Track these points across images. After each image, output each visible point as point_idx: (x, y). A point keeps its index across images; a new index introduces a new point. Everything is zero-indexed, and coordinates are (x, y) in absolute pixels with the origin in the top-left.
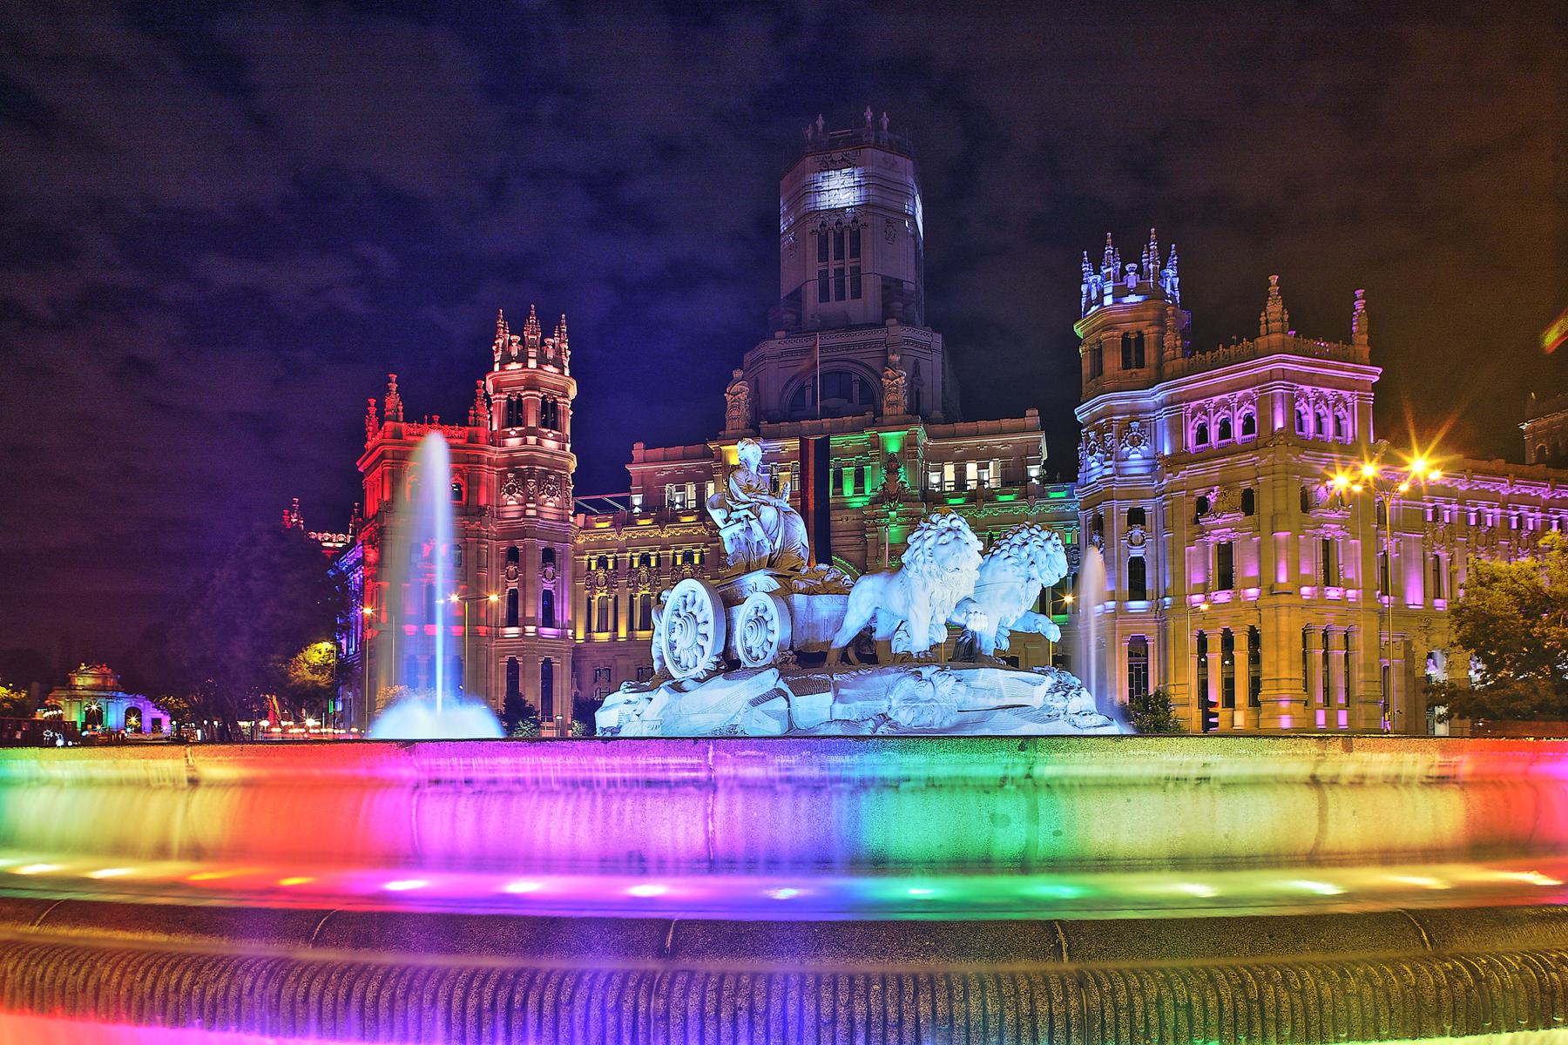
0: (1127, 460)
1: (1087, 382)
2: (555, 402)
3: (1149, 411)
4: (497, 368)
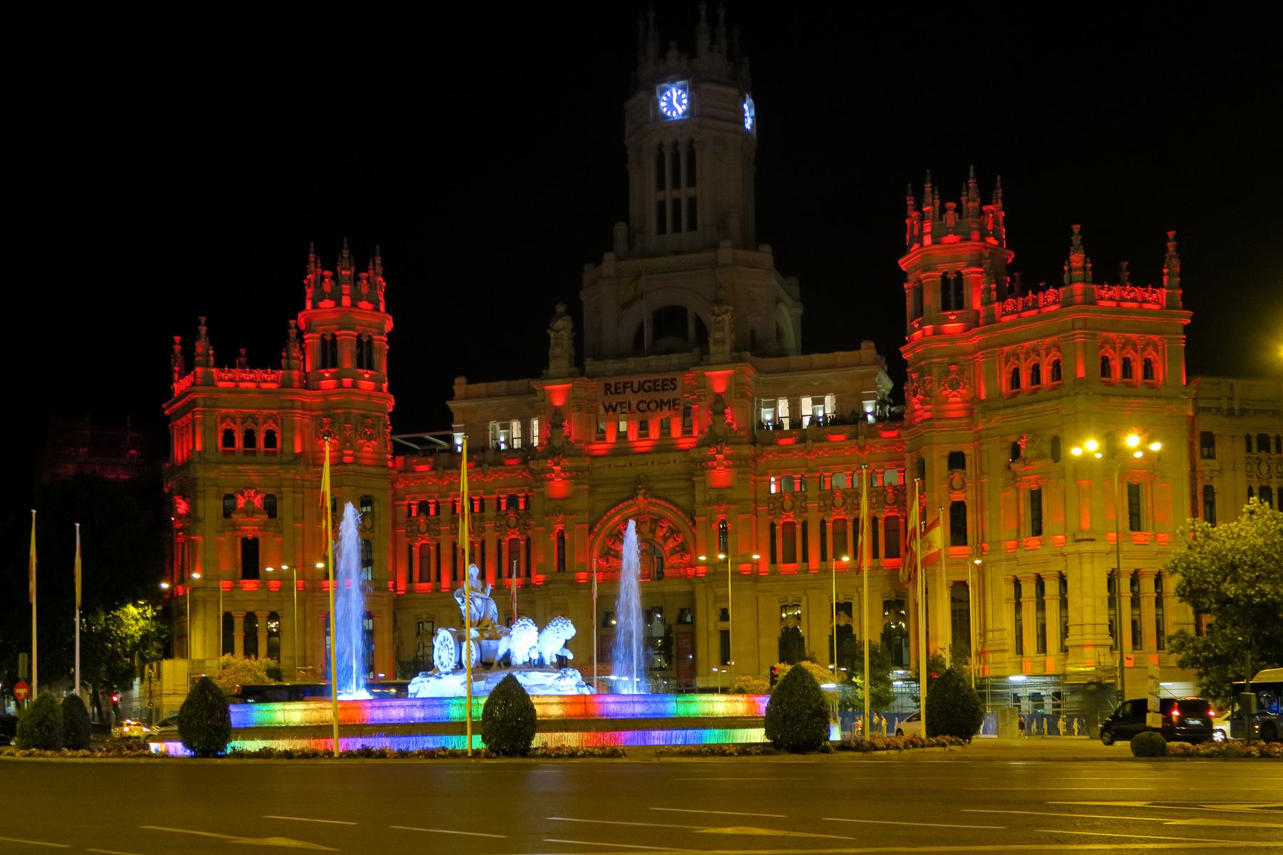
0: (946, 402)
1: (912, 321)
2: (370, 342)
3: (966, 354)
4: (309, 305)
